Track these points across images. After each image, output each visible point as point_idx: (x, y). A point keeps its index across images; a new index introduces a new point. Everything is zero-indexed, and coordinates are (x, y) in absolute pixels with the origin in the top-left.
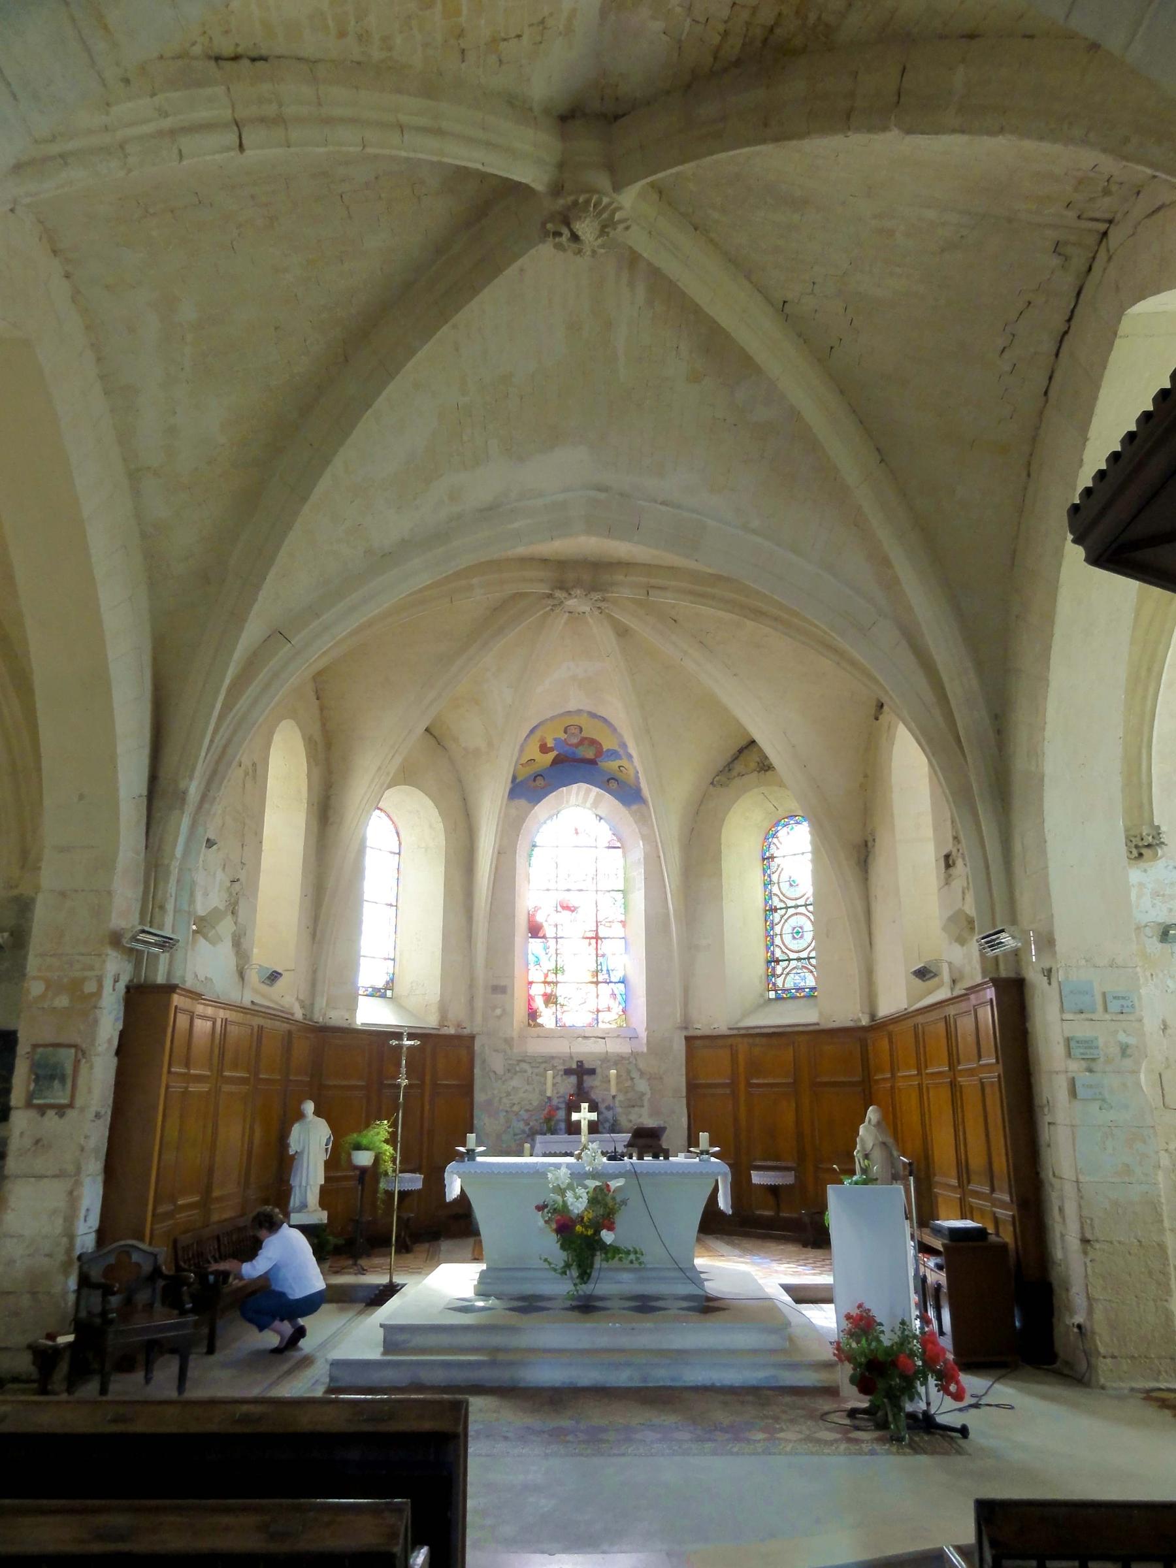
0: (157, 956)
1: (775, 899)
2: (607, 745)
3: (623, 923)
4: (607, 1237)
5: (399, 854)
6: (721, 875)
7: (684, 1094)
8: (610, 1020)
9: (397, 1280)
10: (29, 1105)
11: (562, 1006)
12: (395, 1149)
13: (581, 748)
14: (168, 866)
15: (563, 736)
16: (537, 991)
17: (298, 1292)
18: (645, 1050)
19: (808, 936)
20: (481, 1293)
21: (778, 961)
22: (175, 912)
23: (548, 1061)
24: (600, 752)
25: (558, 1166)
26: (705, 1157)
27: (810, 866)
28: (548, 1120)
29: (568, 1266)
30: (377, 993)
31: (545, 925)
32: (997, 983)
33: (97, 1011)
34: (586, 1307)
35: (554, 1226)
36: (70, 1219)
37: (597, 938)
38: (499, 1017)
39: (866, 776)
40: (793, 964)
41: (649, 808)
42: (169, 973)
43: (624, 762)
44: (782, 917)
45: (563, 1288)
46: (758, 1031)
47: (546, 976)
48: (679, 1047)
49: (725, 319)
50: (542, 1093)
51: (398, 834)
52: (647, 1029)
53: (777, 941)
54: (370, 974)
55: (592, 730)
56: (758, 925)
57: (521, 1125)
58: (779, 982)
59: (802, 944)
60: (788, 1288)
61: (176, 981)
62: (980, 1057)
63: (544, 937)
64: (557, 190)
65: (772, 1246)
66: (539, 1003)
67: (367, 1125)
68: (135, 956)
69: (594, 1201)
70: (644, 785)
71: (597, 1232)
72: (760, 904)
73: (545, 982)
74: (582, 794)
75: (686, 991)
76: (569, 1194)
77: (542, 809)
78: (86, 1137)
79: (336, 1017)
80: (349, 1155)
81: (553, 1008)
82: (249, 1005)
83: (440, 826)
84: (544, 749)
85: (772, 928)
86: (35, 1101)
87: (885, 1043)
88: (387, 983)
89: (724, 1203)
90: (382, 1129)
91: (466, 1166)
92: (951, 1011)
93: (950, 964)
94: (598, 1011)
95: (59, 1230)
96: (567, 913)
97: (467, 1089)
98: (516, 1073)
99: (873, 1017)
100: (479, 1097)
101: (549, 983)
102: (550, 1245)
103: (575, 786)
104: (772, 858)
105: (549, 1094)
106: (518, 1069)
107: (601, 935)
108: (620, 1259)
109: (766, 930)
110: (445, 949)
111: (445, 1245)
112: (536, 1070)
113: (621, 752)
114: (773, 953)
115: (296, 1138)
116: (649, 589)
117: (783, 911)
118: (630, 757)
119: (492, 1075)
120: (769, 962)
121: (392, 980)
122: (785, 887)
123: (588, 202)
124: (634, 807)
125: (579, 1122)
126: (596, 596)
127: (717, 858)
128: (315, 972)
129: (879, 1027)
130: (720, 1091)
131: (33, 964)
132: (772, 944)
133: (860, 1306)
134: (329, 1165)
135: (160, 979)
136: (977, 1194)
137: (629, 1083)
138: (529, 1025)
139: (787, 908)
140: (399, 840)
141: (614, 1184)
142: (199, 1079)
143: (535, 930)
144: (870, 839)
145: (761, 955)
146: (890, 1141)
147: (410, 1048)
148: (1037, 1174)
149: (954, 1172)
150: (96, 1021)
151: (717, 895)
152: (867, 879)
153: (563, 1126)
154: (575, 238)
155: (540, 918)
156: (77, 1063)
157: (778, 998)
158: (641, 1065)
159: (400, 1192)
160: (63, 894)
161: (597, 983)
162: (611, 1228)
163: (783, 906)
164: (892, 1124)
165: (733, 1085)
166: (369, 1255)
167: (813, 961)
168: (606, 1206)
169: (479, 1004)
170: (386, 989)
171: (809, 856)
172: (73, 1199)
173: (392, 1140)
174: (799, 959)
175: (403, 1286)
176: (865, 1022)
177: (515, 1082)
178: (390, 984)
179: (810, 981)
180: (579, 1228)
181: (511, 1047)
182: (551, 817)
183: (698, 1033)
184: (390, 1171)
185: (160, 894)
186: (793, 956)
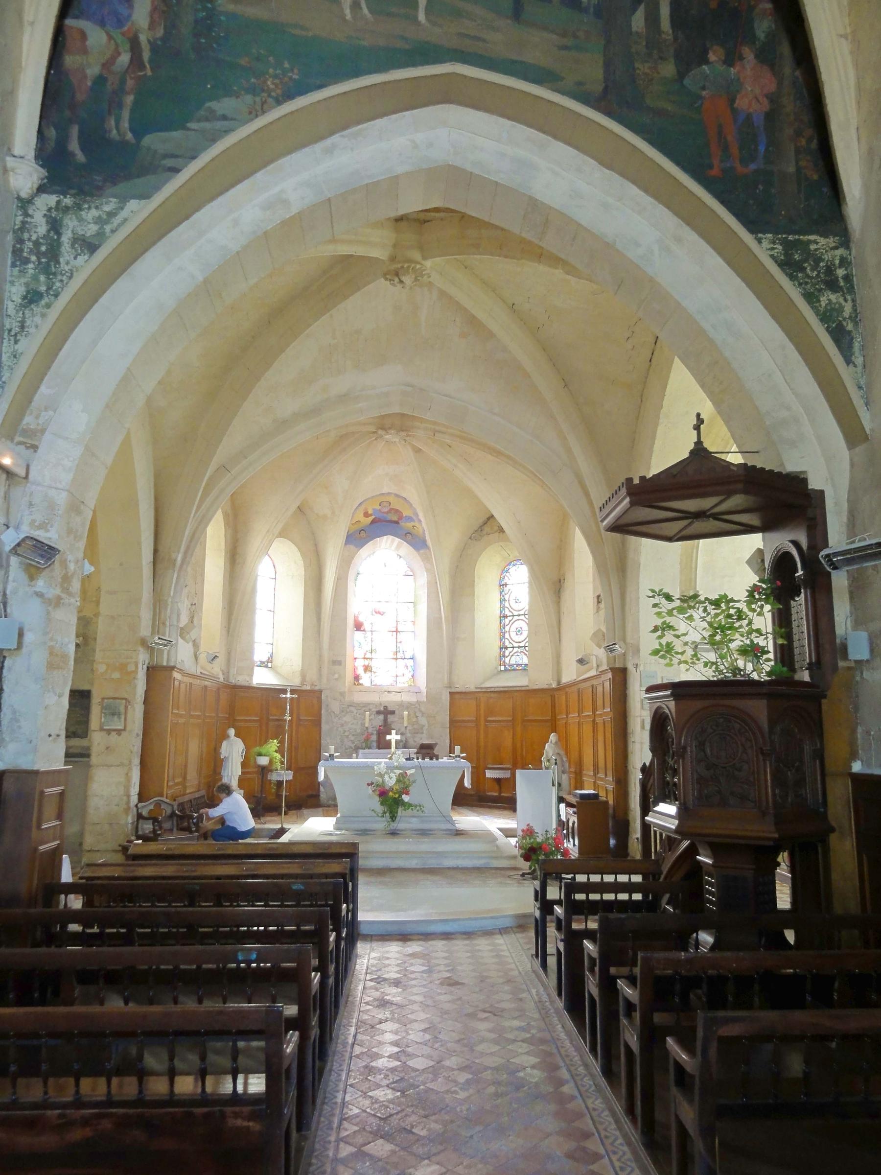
0: (162, 651)
1: (506, 610)
2: (406, 513)
3: (414, 622)
4: (406, 798)
6: (474, 596)
7: (448, 726)
8: (404, 682)
9: (285, 826)
10: (102, 729)
11: (375, 672)
12: (283, 756)
13: (390, 515)
14: (167, 601)
15: (378, 507)
16: (360, 664)
17: (243, 828)
18: (425, 700)
19: (525, 633)
20: (337, 828)
21: (506, 648)
22: (170, 626)
23: (366, 706)
24: (401, 517)
25: (380, 763)
26: (458, 759)
27: (527, 590)
28: (367, 740)
29: (385, 813)
30: (264, 665)
32: (613, 670)
33: (136, 681)
34: (394, 833)
35: (378, 793)
36: (127, 788)
37: (397, 631)
38: (336, 679)
39: (561, 541)
40: (516, 650)
41: (430, 551)
42: (168, 659)
43: (416, 524)
44: (510, 621)
45: (381, 824)
46: (492, 690)
47: (366, 654)
48: (446, 698)
49: (480, 315)
50: (363, 724)
51: (274, 566)
52: (427, 687)
53: (507, 635)
54: (260, 653)
55: (396, 505)
56: (495, 626)
57: (350, 744)
58: (507, 660)
59: (522, 638)
60: (501, 830)
61: (172, 664)
62: (604, 708)
63: (364, 630)
64: (393, 259)
65: (497, 812)
66: (360, 671)
67: (266, 742)
68: (151, 650)
69: (398, 781)
70: (428, 538)
71: (400, 796)
72: (498, 613)
73: (364, 658)
74: (389, 541)
75: (451, 664)
76: (386, 777)
77: (364, 551)
78: (133, 746)
79: (241, 680)
80: (255, 762)
81: (369, 674)
82: (199, 674)
83: (301, 562)
84: (366, 515)
85: (504, 628)
86: (105, 728)
87: (564, 697)
88: (269, 658)
89: (467, 783)
90: (273, 745)
91: (330, 762)
92: (595, 682)
93: (596, 656)
94: (397, 676)
95: (122, 792)
96: (379, 615)
97: (317, 723)
98: (347, 712)
99: (559, 683)
100: (324, 727)
101: (367, 659)
102: (375, 803)
103: (385, 537)
104: (506, 585)
105: (367, 725)
106: (348, 710)
107: (399, 630)
108: (412, 809)
111: (305, 811)
112: (360, 711)
113: (414, 518)
114: (504, 643)
115: (224, 749)
116: (435, 432)
117: (511, 618)
118: (420, 521)
119: (332, 714)
120: (501, 648)
121: (271, 656)
122: (513, 603)
123: (409, 267)
124: (422, 551)
125: (390, 741)
126: (403, 434)
127: (472, 585)
128: (229, 653)
129: (562, 688)
130: (469, 724)
131: (98, 655)
133: (528, 825)
134: (244, 765)
135: (165, 664)
136: (601, 779)
137: (414, 720)
138: (355, 684)
139: (513, 616)
141: (409, 772)
142: (181, 716)
143: (358, 626)
144: (562, 579)
145: (496, 645)
146: (562, 753)
147: (292, 699)
148: (626, 767)
149: (592, 768)
150: (135, 687)
151: (472, 609)
152: (559, 602)
153: (375, 744)
154: (401, 282)
155: (361, 619)
156: (126, 707)
157: (506, 670)
158: (423, 709)
159: (286, 781)
160: (113, 617)
161: (396, 659)
162: (407, 794)
163: (511, 614)
164: (564, 743)
165: (477, 721)
166: (263, 816)
167: (527, 648)
168: (405, 783)
169: (325, 671)
170: (268, 662)
171: (527, 585)
172: (128, 778)
173: (280, 751)
174: (519, 647)
175: (289, 829)
176: (554, 686)
177: (347, 718)
178: (270, 660)
179: (525, 660)
180: (391, 794)
181: (344, 698)
182: (369, 556)
183: (458, 690)
184: (279, 768)
185: (162, 616)
186: (516, 645)
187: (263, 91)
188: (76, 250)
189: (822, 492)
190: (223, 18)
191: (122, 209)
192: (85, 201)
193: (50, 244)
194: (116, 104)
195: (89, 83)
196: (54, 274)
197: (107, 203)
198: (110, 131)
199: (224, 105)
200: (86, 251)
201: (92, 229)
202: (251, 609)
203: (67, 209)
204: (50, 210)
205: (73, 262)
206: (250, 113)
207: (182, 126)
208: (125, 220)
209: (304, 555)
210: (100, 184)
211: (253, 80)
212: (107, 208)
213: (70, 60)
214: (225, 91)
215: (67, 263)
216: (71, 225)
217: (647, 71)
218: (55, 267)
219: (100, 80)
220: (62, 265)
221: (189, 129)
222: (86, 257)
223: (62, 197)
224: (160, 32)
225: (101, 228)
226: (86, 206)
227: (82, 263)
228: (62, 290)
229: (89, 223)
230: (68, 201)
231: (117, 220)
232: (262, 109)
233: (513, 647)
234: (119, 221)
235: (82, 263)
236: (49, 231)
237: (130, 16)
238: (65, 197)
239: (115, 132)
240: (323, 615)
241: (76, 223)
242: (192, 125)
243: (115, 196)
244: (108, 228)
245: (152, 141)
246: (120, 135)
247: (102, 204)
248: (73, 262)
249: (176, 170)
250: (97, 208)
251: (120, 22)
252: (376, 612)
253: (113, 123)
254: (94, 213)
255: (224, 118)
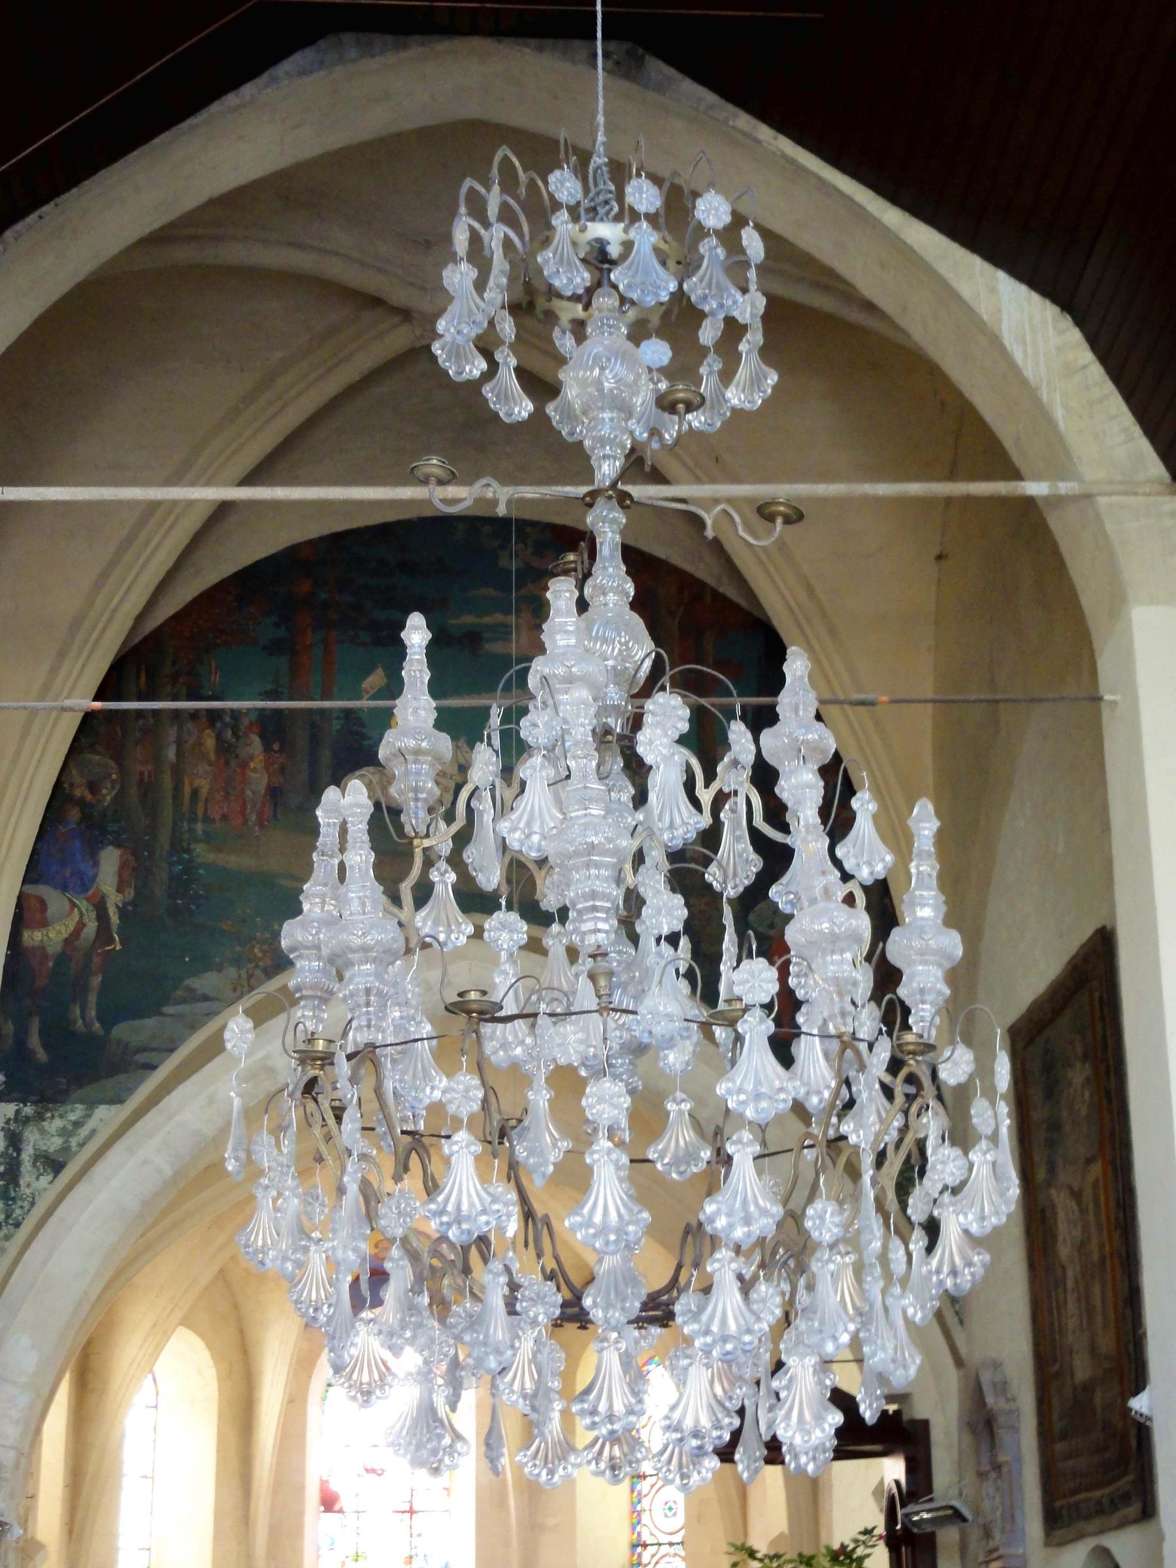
5: (156, 1407)
19: (680, 1520)
21: (645, 1546)
31: (341, 1494)
37: (412, 1512)
40: (665, 1549)
44: (652, 1486)
53: (645, 1518)
85: (639, 1502)
107: (415, 1508)
109: (632, 1503)
110: (217, 1538)
114: (639, 1534)
120: (634, 1546)
132: (639, 1522)
140: (156, 1388)
143: (329, 1502)
145: (624, 1538)
155: (334, 1486)
174: (671, 1544)
187: (250, 961)
188: (38, 1170)
189: (925, 1424)
190: (201, 871)
191: (89, 1116)
192: (47, 1110)
193: (8, 1163)
194: (80, 989)
195: (51, 964)
196: (13, 1199)
197: (72, 1111)
198: (75, 1023)
199: (205, 982)
200: (49, 1170)
201: (55, 1144)
202: (110, 1478)
203: (27, 1120)
204: (8, 1122)
205: (35, 1184)
206: (235, 990)
207: (156, 1011)
208: (94, 1132)
209: (217, 1355)
210: (64, 1087)
211: (238, 948)
212: (73, 1117)
213: (32, 937)
214: (204, 964)
215: (28, 1186)
216: (32, 1140)
217: (703, 907)
218: (15, 1191)
219: (63, 958)
220: (22, 1188)
221: (164, 1015)
222: (50, 1178)
223: (21, 1105)
224: (130, 893)
225: (66, 1141)
226: (49, 1115)
227: (46, 1185)
228: (23, 1219)
229: (53, 1136)
230: (29, 1110)
231: (84, 1132)
232: (249, 986)
233: (660, 1545)
234: (87, 1133)
235: (46, 1185)
236: (7, 1148)
237: (95, 876)
238: (26, 1106)
239: (80, 1022)
240: (255, 1484)
241: (37, 1136)
242: (168, 1010)
243: (82, 1102)
244: (74, 1142)
245: (121, 1031)
246: (86, 1026)
247: (66, 1112)
248: (35, 1184)
249: (153, 1067)
250: (61, 1116)
251: (84, 883)
252: (367, 1470)
253: (78, 1012)
254: (58, 1123)
255: (206, 998)
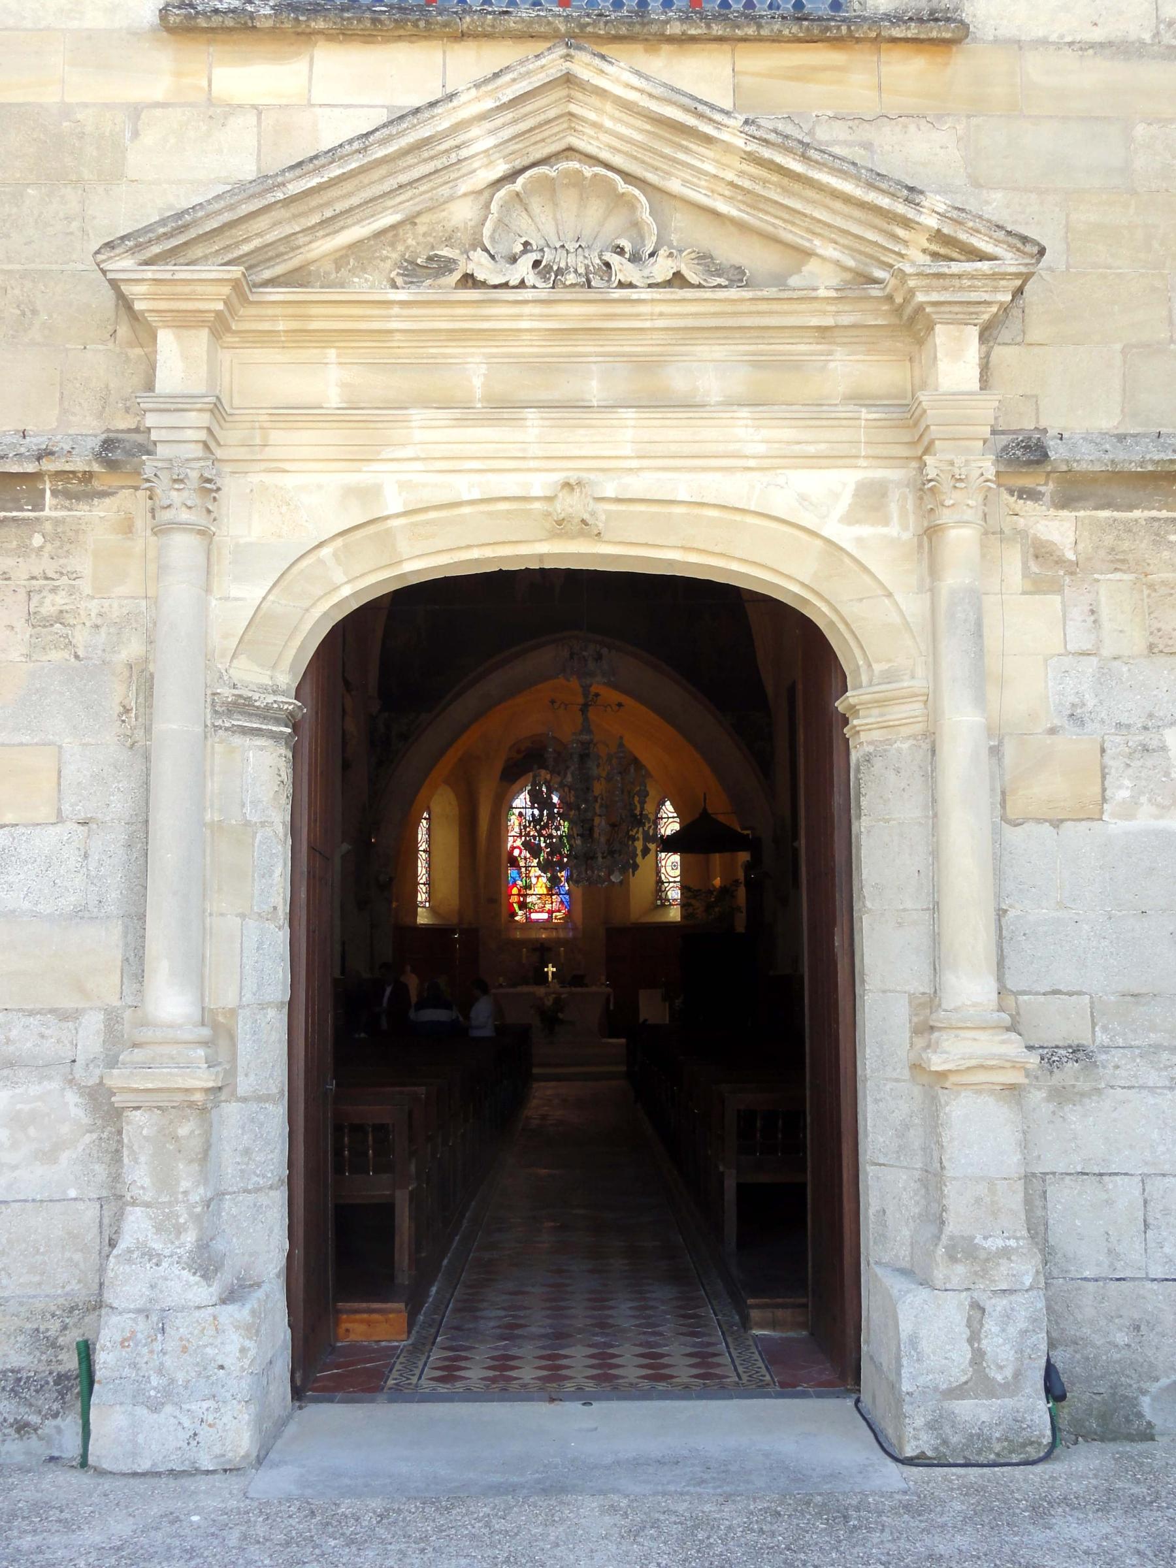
4: (560, 1016)
23: (523, 943)
40: (671, 885)
47: (520, 890)
53: (663, 870)
83: (454, 802)
89: (612, 1007)
91: (501, 991)
110: (461, 878)
145: (653, 878)
161: (552, 895)
233: (669, 882)
